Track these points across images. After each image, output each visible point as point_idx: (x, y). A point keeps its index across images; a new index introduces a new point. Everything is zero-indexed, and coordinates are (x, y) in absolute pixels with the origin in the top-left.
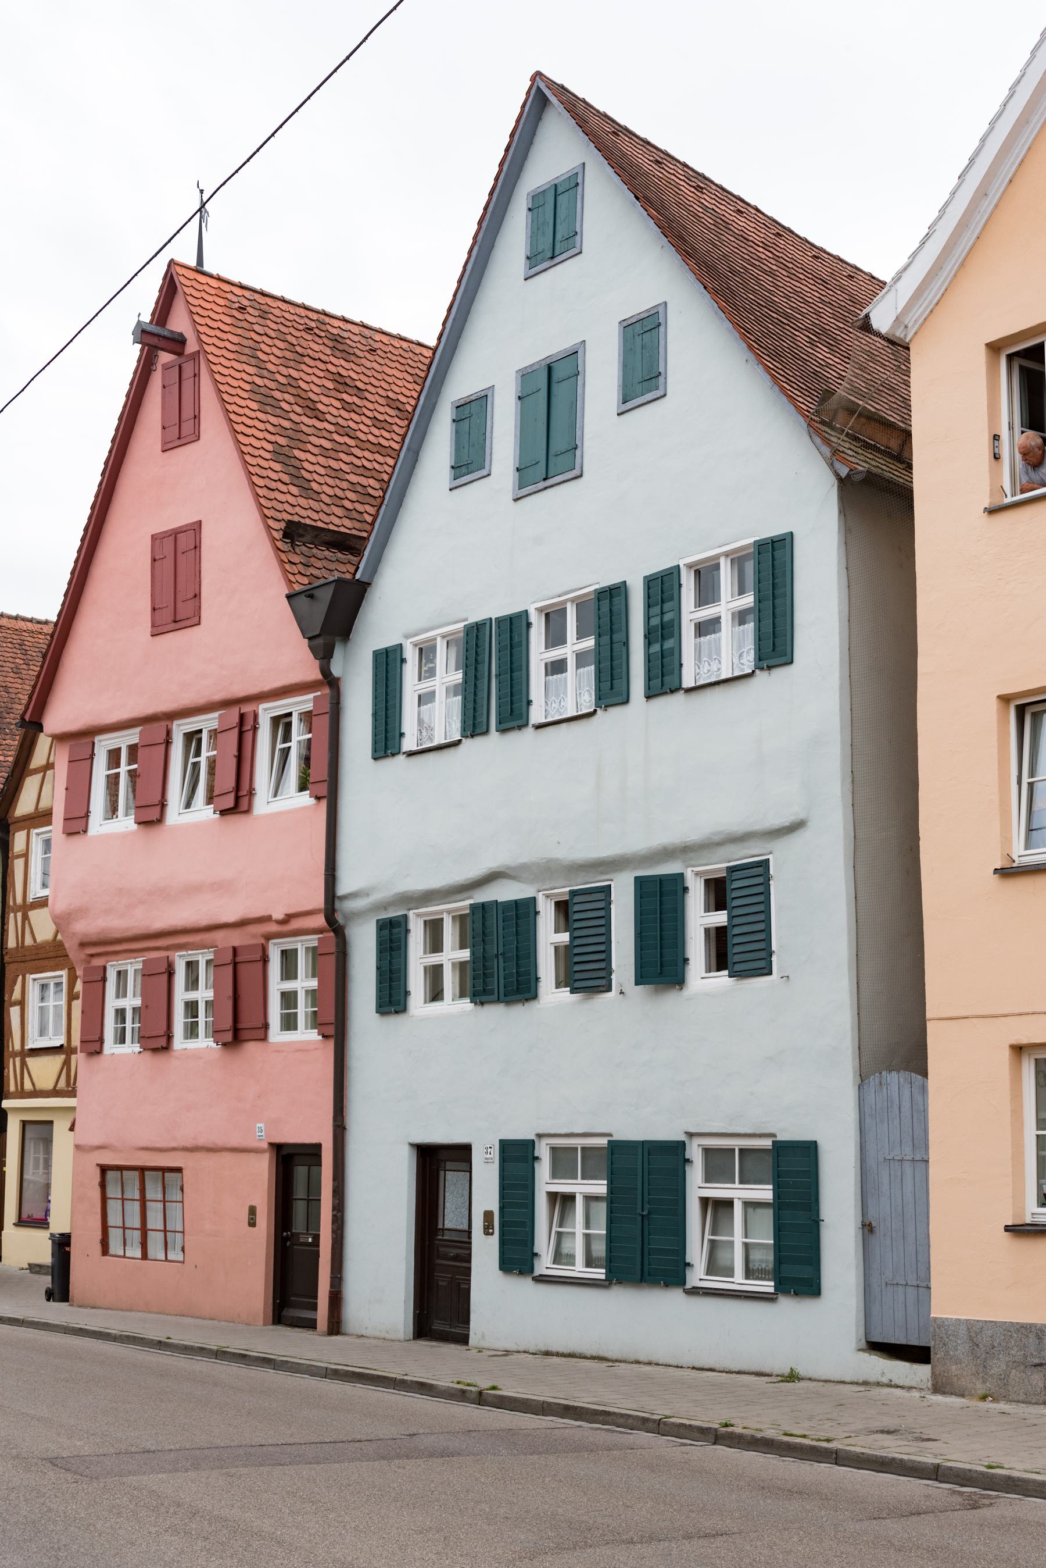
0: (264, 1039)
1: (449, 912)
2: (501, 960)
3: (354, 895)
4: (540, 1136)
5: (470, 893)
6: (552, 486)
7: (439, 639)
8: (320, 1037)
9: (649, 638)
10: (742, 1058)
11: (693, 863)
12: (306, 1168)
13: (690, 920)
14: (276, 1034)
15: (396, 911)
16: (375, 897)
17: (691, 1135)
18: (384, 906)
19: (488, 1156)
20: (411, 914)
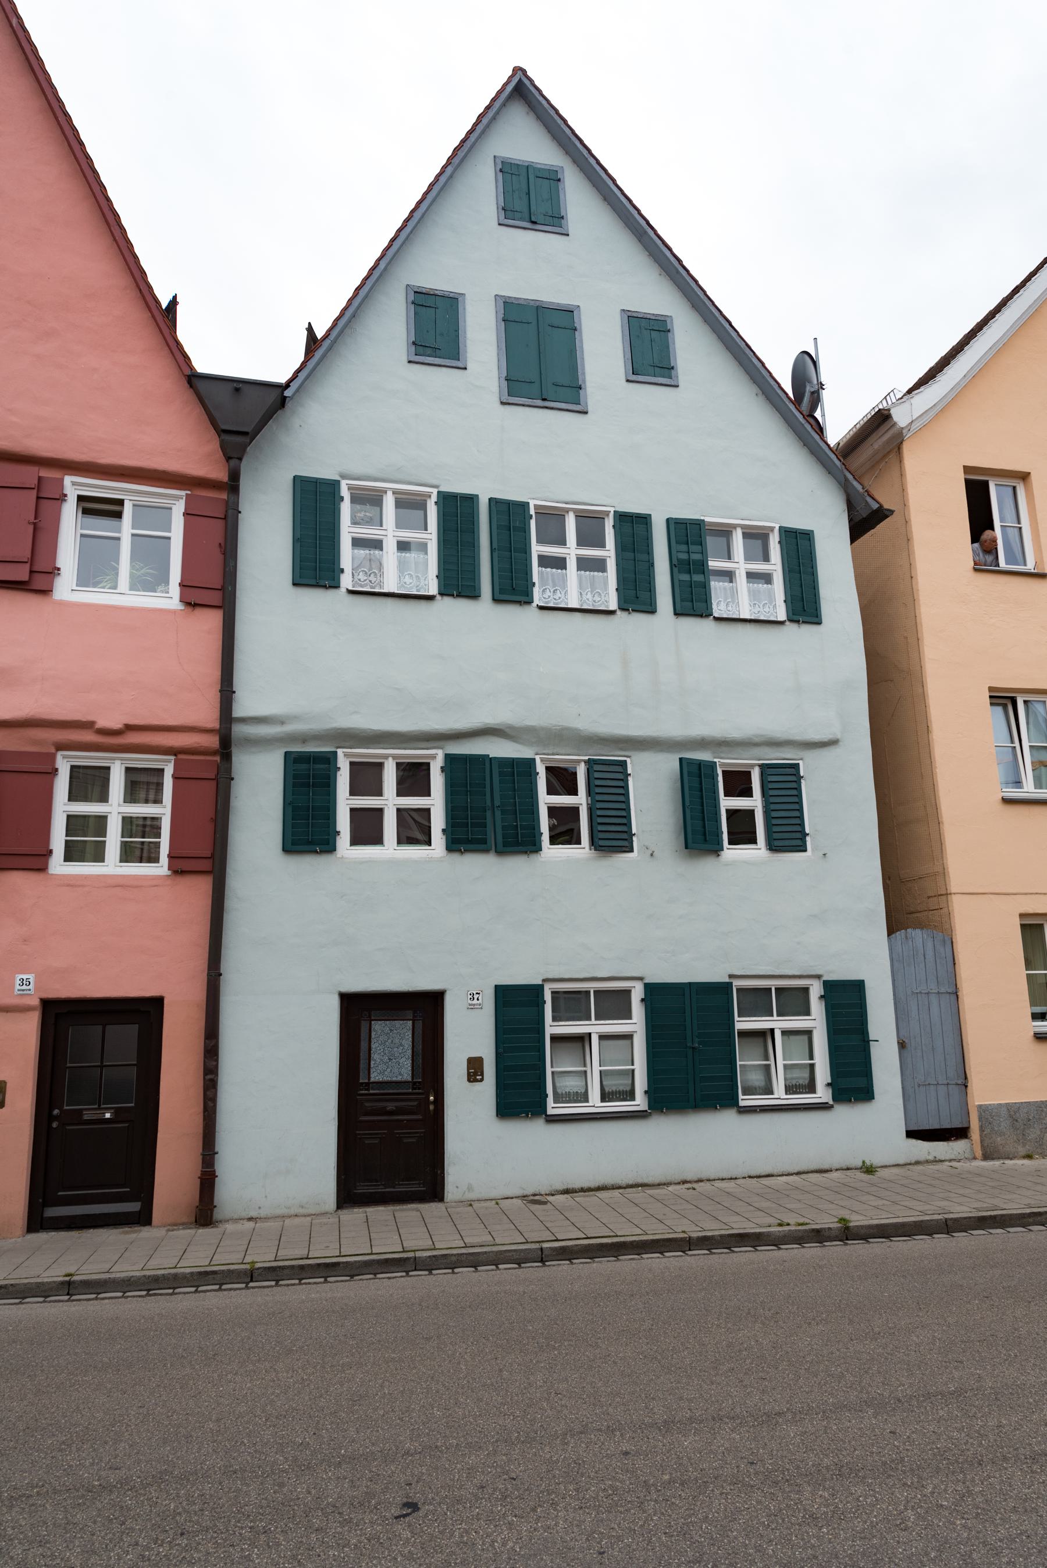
0: (43, 869)
1: (394, 757)
2: (498, 813)
3: (243, 720)
4: (544, 980)
5: (441, 743)
6: (552, 408)
7: (390, 493)
8: (169, 873)
9: (676, 566)
10: (796, 914)
11: (723, 755)
12: (100, 1028)
13: (736, 802)
14: (58, 865)
15: (319, 746)
16: (289, 728)
17: (730, 976)
18: (304, 738)
19: (475, 1002)
20: (340, 752)
